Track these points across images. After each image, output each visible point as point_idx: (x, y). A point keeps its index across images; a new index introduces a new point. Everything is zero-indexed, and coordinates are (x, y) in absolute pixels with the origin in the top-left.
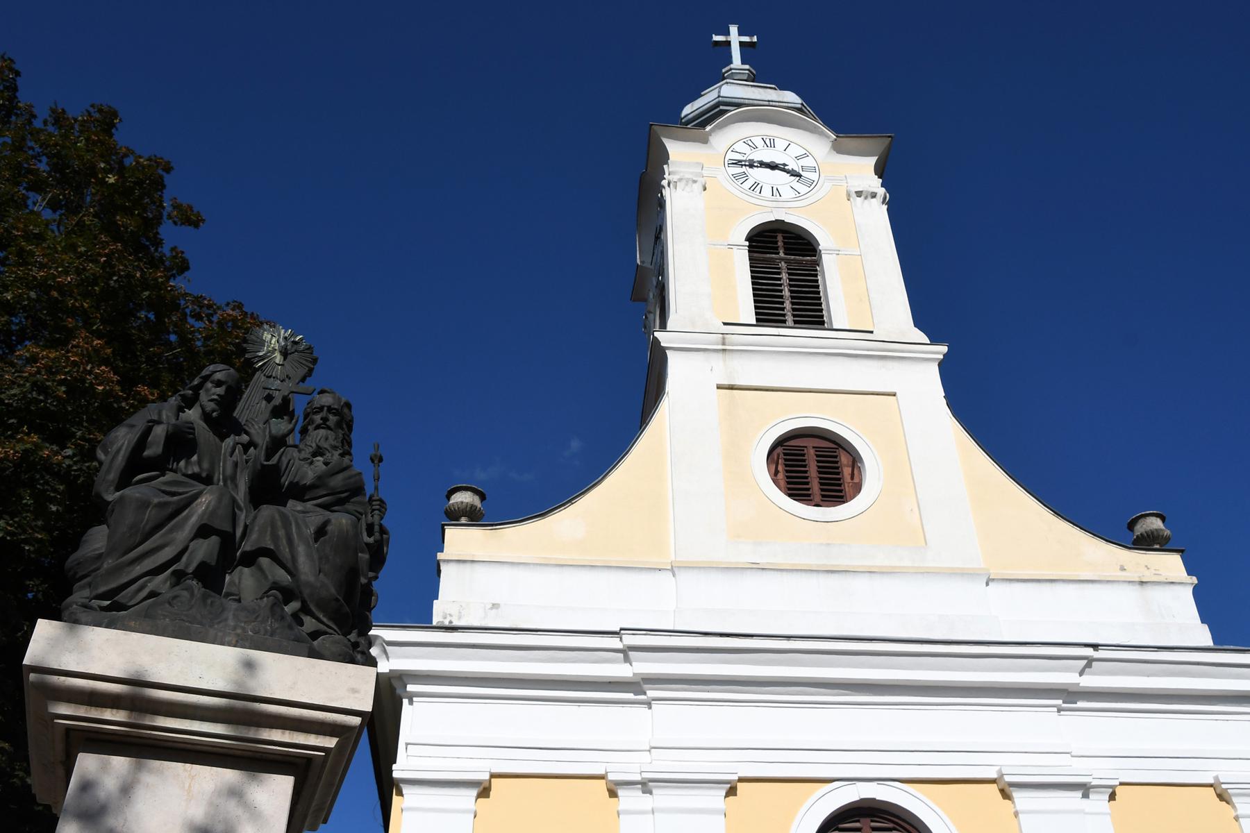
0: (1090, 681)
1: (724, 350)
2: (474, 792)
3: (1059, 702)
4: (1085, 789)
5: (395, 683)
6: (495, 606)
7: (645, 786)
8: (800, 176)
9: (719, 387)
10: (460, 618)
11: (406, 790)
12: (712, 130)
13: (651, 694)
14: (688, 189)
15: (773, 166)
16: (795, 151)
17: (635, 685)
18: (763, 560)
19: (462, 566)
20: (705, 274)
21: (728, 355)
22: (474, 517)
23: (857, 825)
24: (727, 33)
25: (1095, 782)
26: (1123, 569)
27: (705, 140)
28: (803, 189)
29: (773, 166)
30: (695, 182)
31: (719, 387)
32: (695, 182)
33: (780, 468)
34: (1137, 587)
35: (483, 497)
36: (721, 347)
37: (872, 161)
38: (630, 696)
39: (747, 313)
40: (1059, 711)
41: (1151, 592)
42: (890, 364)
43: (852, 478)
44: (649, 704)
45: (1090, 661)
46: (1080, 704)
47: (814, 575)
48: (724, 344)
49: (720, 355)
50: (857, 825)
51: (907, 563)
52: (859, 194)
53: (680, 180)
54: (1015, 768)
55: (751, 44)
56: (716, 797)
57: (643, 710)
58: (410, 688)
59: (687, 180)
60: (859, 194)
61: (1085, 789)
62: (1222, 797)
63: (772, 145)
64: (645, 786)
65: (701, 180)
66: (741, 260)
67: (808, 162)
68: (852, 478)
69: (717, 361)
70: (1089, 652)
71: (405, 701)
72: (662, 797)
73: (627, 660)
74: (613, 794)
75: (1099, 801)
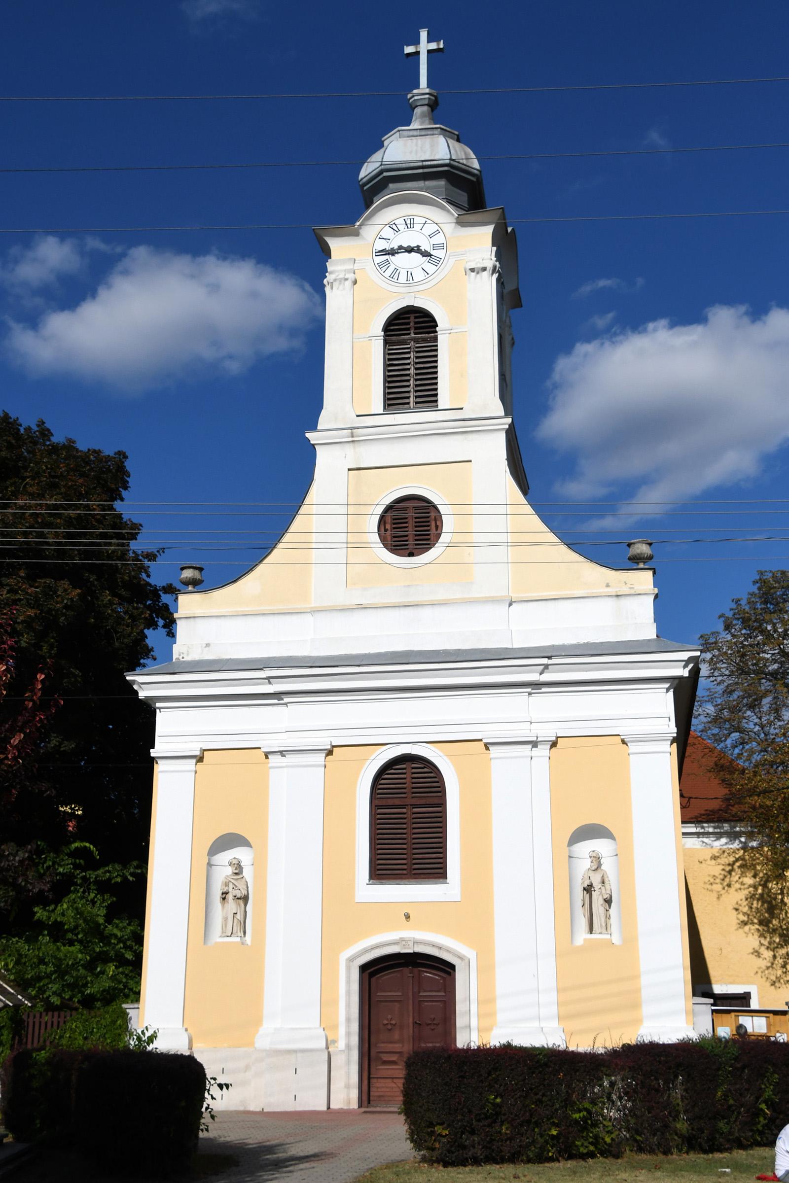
0: (547, 677)
1: (353, 441)
2: (194, 761)
3: (529, 690)
4: (534, 744)
5: (150, 702)
6: (208, 645)
7: (282, 753)
8: (430, 255)
9: (349, 470)
10: (188, 654)
11: (159, 761)
12: (360, 225)
13: (286, 700)
14: (341, 287)
15: (410, 250)
16: (430, 228)
17: (278, 695)
18: (364, 602)
19: (189, 620)
20: (353, 365)
21: (356, 443)
22: (196, 585)
23: (404, 766)
24: (417, 42)
25: (539, 739)
26: (608, 586)
27: (356, 234)
28: (431, 268)
29: (410, 250)
30: (346, 279)
31: (349, 470)
32: (346, 279)
33: (388, 527)
34: (615, 598)
35: (200, 569)
36: (351, 439)
37: (489, 230)
38: (276, 701)
39: (377, 402)
40: (530, 694)
41: (624, 602)
42: (470, 436)
43: (437, 530)
44: (286, 704)
45: (546, 666)
46: (544, 690)
47: (397, 609)
48: (353, 437)
49: (351, 444)
50: (404, 766)
51: (458, 596)
52: (472, 270)
53: (335, 280)
54: (489, 733)
55: (439, 50)
56: (320, 758)
57: (284, 707)
58: (158, 705)
59: (340, 280)
60: (472, 270)
61: (534, 744)
62: (623, 742)
63: (409, 225)
64: (282, 753)
65: (351, 276)
66: (377, 349)
67: (439, 239)
68: (437, 530)
69: (349, 450)
70: (545, 661)
71: (158, 711)
72: (290, 759)
73: (270, 683)
74: (267, 757)
75: (543, 751)
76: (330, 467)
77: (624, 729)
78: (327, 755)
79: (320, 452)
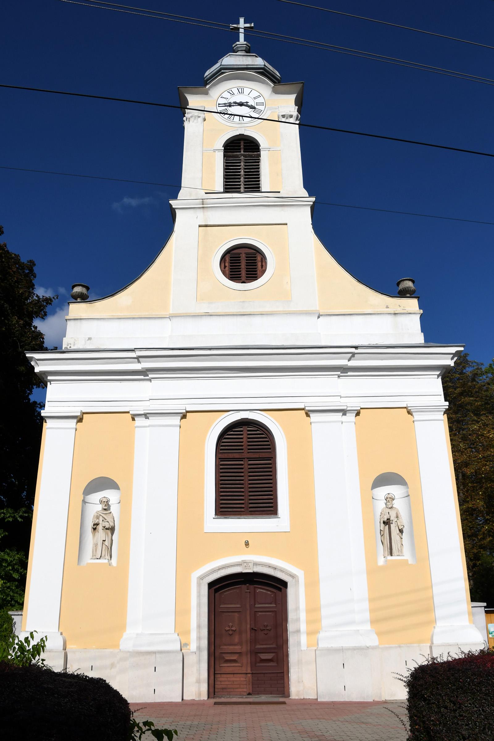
0: (353, 363)
1: (203, 207)
2: (75, 421)
3: (339, 373)
4: (344, 412)
5: (43, 376)
6: (90, 339)
7: (146, 416)
8: (255, 108)
9: (200, 226)
10: (74, 345)
12: (210, 87)
13: (151, 376)
14: (195, 121)
15: (241, 104)
17: (144, 372)
18: (210, 311)
19: (76, 321)
22: (83, 298)
23: (242, 429)
25: (348, 409)
26: (387, 307)
27: (206, 93)
29: (241, 104)
30: (199, 117)
31: (200, 226)
32: (199, 117)
33: (227, 264)
34: (393, 316)
35: (88, 288)
36: (201, 206)
37: (293, 97)
38: (142, 377)
40: (339, 377)
42: (286, 209)
43: (262, 268)
44: (150, 380)
45: (353, 354)
46: (349, 374)
47: (235, 317)
48: (203, 204)
49: (202, 210)
50: (242, 429)
51: (280, 309)
53: (192, 117)
54: (310, 403)
56: (176, 420)
57: (148, 383)
58: (49, 378)
59: (195, 117)
61: (344, 412)
62: (409, 412)
64: (146, 416)
67: (261, 100)
68: (262, 268)
69: (200, 213)
70: (353, 350)
71: (49, 383)
72: (153, 420)
73: (139, 362)
74: (133, 419)
75: (351, 417)
76: (185, 224)
77: (411, 402)
78: (182, 418)
79: (179, 215)
